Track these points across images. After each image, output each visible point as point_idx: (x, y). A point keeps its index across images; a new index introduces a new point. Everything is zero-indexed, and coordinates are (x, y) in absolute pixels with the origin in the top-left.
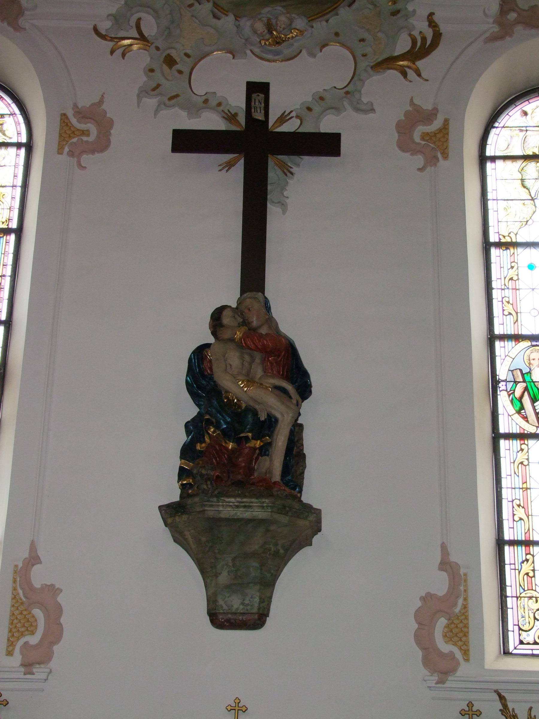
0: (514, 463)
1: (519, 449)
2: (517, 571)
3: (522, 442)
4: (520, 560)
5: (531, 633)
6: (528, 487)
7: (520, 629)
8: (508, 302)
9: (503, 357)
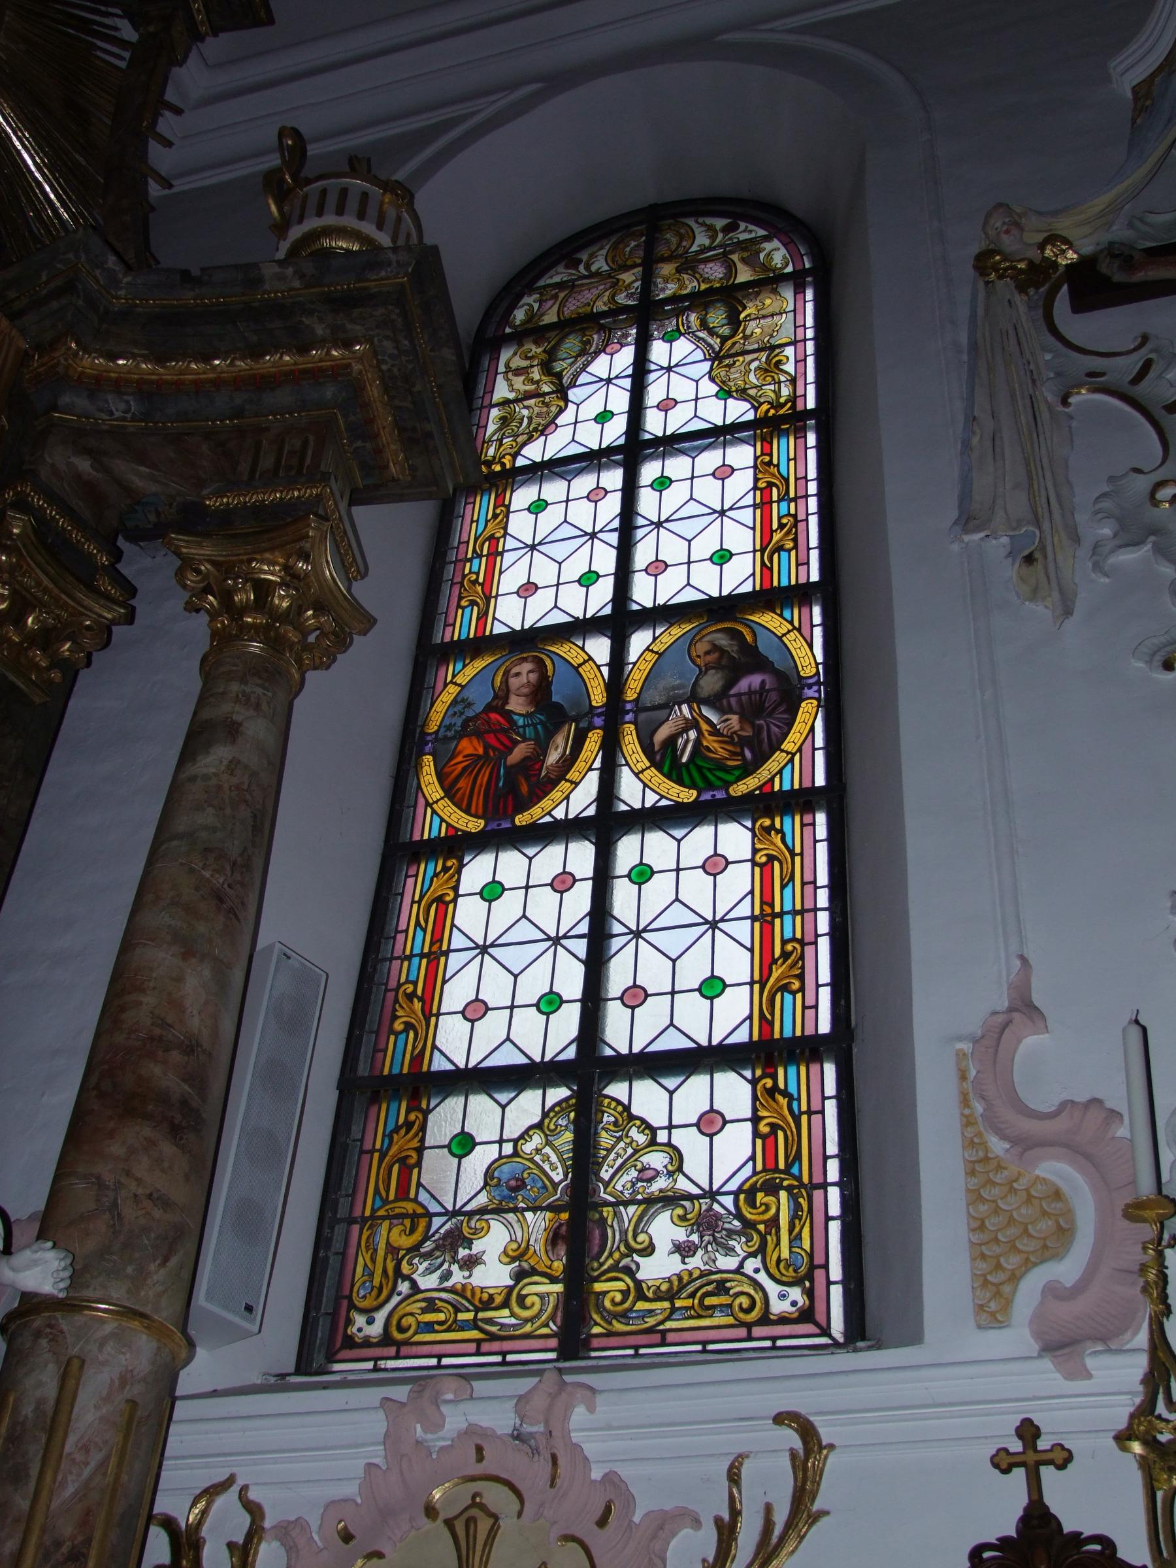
0: (419, 902)
2: (376, 1155)
4: (391, 1126)
5: (381, 1316)
8: (476, 581)
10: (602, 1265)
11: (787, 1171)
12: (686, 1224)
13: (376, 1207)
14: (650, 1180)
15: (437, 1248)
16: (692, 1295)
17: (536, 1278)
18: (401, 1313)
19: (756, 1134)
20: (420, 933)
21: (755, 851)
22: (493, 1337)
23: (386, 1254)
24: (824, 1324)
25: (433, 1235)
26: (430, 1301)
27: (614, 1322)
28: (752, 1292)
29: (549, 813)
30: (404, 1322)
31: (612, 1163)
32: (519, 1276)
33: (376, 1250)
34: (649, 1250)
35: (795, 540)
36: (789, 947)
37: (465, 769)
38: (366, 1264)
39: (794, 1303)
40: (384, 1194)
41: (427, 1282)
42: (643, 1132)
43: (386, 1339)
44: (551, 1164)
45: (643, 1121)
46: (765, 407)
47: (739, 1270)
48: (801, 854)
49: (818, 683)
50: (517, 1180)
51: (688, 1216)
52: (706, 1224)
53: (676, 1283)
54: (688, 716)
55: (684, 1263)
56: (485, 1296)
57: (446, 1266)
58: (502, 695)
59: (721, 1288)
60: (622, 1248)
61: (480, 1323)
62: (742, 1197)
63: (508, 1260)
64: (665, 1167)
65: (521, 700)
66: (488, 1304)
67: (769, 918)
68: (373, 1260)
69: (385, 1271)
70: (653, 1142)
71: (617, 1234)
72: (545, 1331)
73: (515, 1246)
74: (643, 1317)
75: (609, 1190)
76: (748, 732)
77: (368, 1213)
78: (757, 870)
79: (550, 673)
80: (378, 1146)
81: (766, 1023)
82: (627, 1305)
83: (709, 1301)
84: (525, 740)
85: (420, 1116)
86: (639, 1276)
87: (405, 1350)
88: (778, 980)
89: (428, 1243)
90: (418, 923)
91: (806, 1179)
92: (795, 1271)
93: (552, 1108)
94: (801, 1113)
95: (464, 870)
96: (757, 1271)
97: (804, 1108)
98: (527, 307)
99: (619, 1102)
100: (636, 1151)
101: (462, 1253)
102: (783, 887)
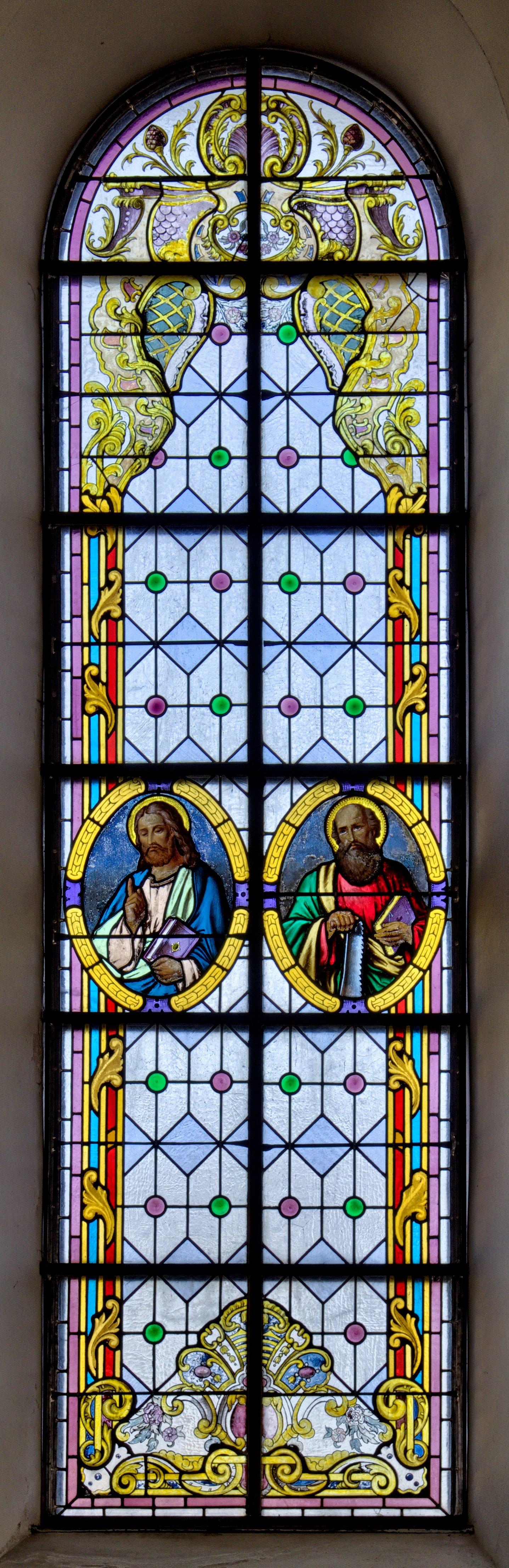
0: (90, 1083)
1: (103, 1049)
2: (83, 1338)
3: (112, 1033)
4: (92, 1312)
6: (120, 1139)
7: (81, 1464)
8: (97, 679)
9: (77, 823)
13: (89, 1383)
16: (343, 1472)
19: (389, 1347)
21: (389, 1075)
22: (195, 1495)
24: (437, 1501)
29: (202, 1001)
30: (125, 1481)
32: (213, 1448)
33: (93, 1419)
34: (310, 1433)
39: (416, 1484)
40: (94, 1372)
42: (302, 1335)
43: (113, 1494)
45: (302, 1326)
46: (395, 495)
48: (428, 1084)
55: (336, 1446)
63: (201, 1435)
67: (401, 1147)
68: (93, 1427)
69: (103, 1439)
72: (236, 1492)
78: (391, 1094)
80: (83, 1329)
81: (399, 1249)
83: (355, 1477)
85: (117, 1305)
87: (127, 1502)
91: (427, 1390)
94: (424, 1332)
97: (427, 1328)
99: (282, 1308)
102: (412, 1117)
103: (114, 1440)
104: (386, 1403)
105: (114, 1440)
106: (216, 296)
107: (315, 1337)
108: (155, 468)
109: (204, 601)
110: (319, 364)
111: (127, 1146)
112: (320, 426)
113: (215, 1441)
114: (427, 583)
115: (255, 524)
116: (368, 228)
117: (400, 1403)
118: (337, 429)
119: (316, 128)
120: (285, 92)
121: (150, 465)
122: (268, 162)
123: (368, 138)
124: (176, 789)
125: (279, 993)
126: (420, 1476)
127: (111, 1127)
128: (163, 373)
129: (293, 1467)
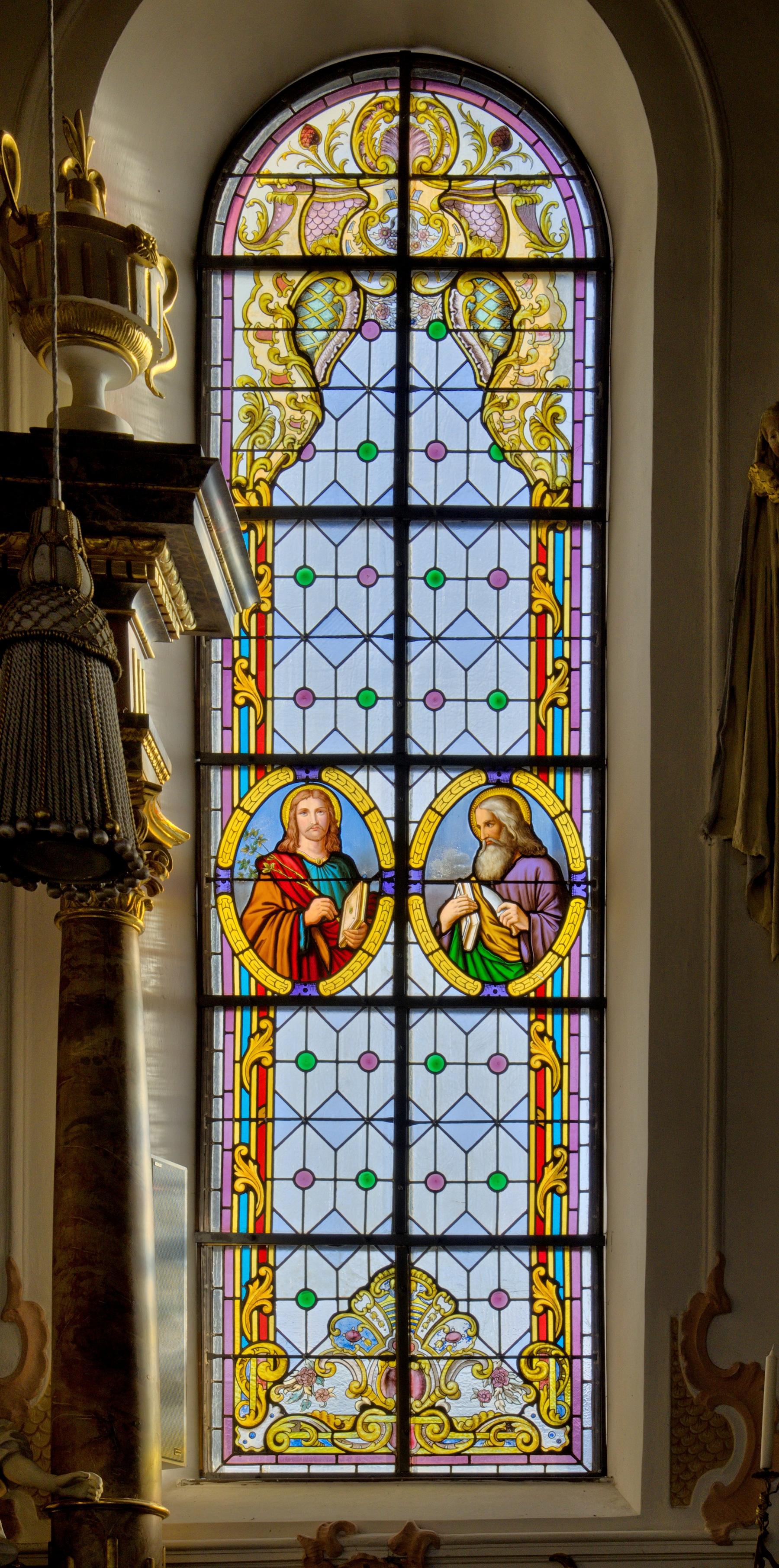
1: (254, 1030)
2: (237, 1302)
3: (264, 1014)
4: (246, 1279)
5: (260, 1432)
10: (422, 1404)
11: (555, 1343)
12: (483, 1377)
14: (455, 1341)
15: (297, 1382)
16: (489, 1431)
17: (375, 1411)
18: (276, 1430)
19: (532, 1312)
20: (245, 1095)
22: (348, 1453)
23: (257, 1384)
25: (292, 1372)
26: (296, 1422)
27: (434, 1446)
28: (530, 1431)
31: (426, 1325)
32: (364, 1408)
33: (248, 1381)
34: (457, 1395)
35: (568, 694)
36: (558, 1152)
37: (266, 919)
38: (242, 1392)
41: (292, 1408)
43: (267, 1451)
44: (379, 1322)
45: (448, 1293)
46: (540, 489)
47: (520, 1415)
49: (585, 882)
50: (354, 1331)
51: (485, 1372)
52: (497, 1378)
53: (477, 1421)
54: (471, 897)
56: (338, 1423)
57: (305, 1397)
58: (291, 833)
59: (509, 1427)
60: (437, 1392)
61: (336, 1441)
62: (523, 1360)
63: (353, 1395)
64: (466, 1331)
65: (312, 845)
66: (340, 1428)
69: (258, 1398)
70: (456, 1311)
71: (433, 1384)
72: (385, 1450)
73: (357, 1385)
74: (455, 1444)
75: (425, 1346)
76: (524, 926)
77: (237, 1352)
78: (533, 1073)
79: (338, 817)
80: (238, 1295)
81: (540, 1220)
82: (442, 1435)
83: (501, 1435)
84: (321, 895)
86: (450, 1414)
88: (549, 1182)
89: (289, 1378)
90: (242, 1086)
91: (568, 1353)
92: (560, 1418)
93: (376, 1274)
94: (565, 1299)
95: (278, 1034)
96: (533, 1416)
97: (568, 1295)
98: (257, 208)
99: (429, 1276)
100: (443, 1317)
101: (317, 1387)
103: (269, 1400)
104: (530, 1366)
105: (269, 1400)
106: (366, 293)
107: (460, 1303)
108: (305, 461)
109: (351, 594)
110: (468, 361)
111: (276, 1122)
112: (468, 421)
113: (366, 1401)
114: (570, 579)
115: (402, 515)
116: (515, 226)
117: (542, 1364)
118: (485, 425)
119: (464, 129)
120: (433, 93)
121: (298, 459)
122: (418, 158)
123: (516, 139)
124: (325, 776)
125: (427, 975)
126: (561, 1434)
127: (262, 1103)
128: (313, 368)
129: (441, 1426)
